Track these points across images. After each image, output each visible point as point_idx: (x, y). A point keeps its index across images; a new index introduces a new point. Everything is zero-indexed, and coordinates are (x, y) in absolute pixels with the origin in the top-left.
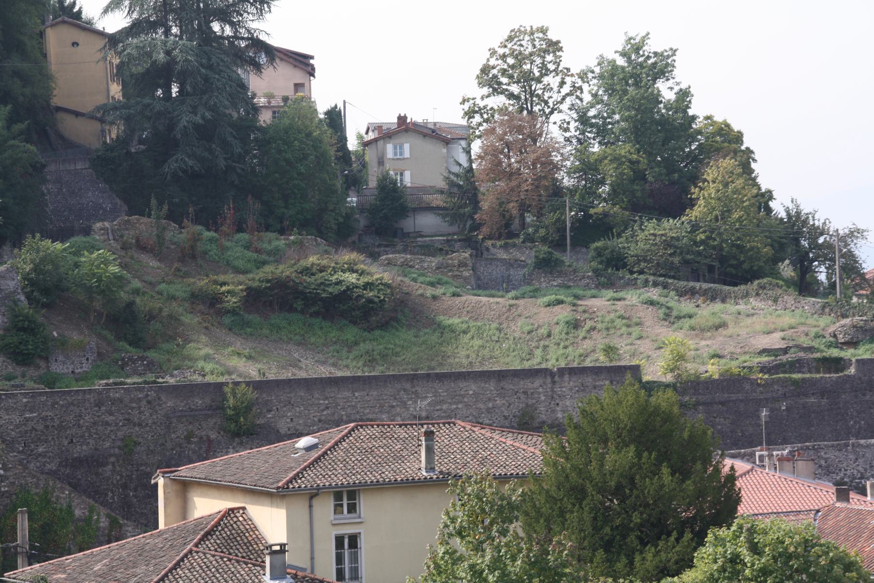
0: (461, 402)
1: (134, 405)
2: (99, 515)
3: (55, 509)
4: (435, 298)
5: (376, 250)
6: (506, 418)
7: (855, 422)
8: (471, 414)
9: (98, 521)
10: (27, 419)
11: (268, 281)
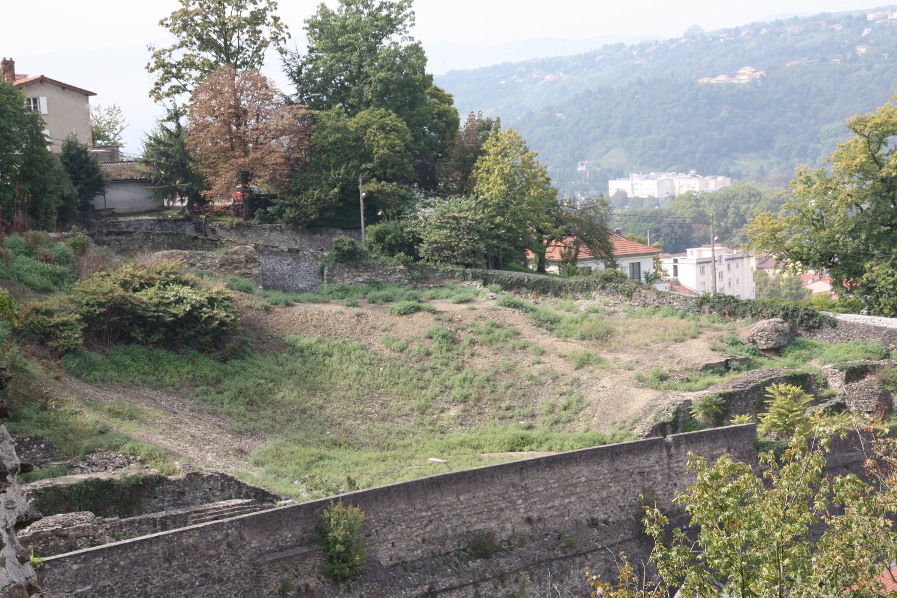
0: (574, 494)
1: (212, 552)
4: (267, 310)
8: (585, 509)
11: (100, 305)
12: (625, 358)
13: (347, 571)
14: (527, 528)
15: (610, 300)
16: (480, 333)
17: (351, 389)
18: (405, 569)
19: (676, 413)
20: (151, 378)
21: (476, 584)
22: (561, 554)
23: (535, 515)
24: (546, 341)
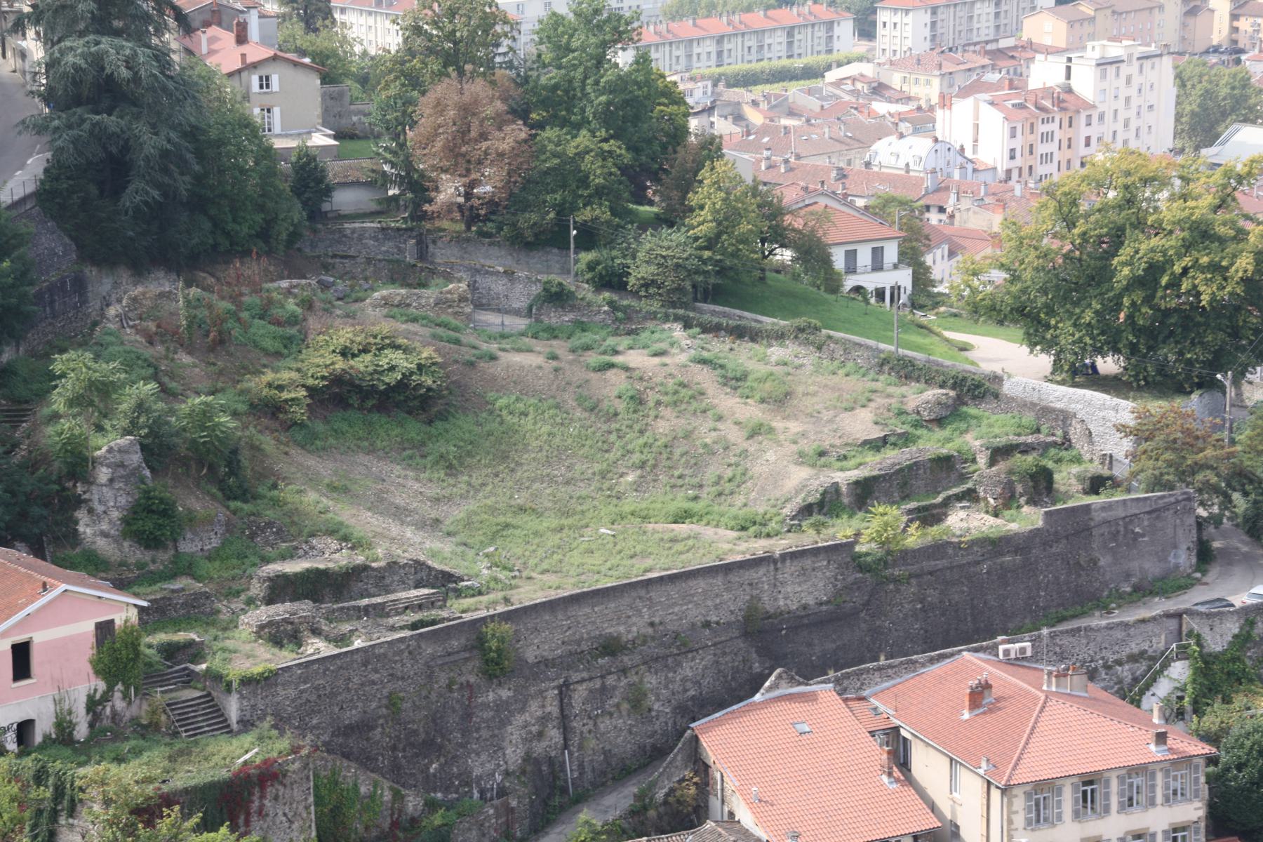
0: (690, 602)
2: (382, 789)
3: (342, 790)
5: (330, 261)
6: (732, 612)
7: (1045, 576)
9: (382, 795)
10: (301, 692)
11: (323, 378)
12: (795, 427)
13: (498, 672)
14: (650, 630)
15: (802, 350)
16: (666, 394)
17: (541, 451)
18: (546, 666)
19: (824, 494)
20: (366, 444)
21: (602, 677)
22: (675, 651)
23: (657, 620)
24: (728, 402)
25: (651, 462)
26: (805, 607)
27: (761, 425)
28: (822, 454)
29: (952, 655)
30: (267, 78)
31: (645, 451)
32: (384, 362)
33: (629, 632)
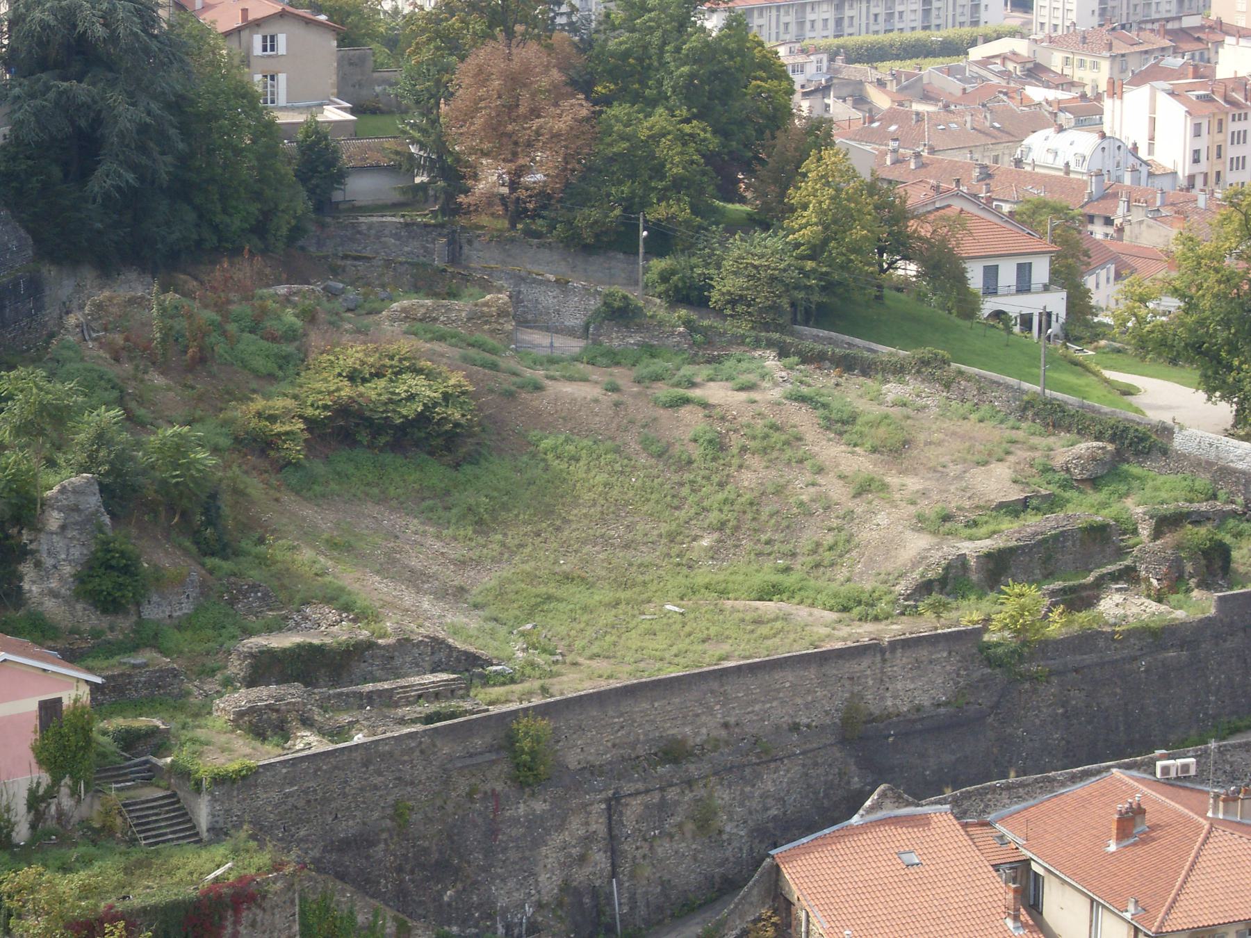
1: (406, 758)
2: (384, 919)
3: (335, 918)
5: (339, 262)
8: (787, 713)
9: (383, 925)
10: (287, 796)
11: (325, 407)
12: (913, 484)
13: (531, 780)
14: (723, 733)
15: (926, 388)
16: (754, 438)
17: (594, 505)
18: (592, 773)
19: (947, 569)
20: (376, 490)
21: (662, 789)
22: (754, 760)
23: (732, 720)
24: (831, 451)
25: (733, 523)
26: (918, 709)
27: (872, 479)
28: (946, 518)
29: (1099, 772)
30: (272, 38)
31: (726, 508)
32: (401, 389)
33: (697, 734)
